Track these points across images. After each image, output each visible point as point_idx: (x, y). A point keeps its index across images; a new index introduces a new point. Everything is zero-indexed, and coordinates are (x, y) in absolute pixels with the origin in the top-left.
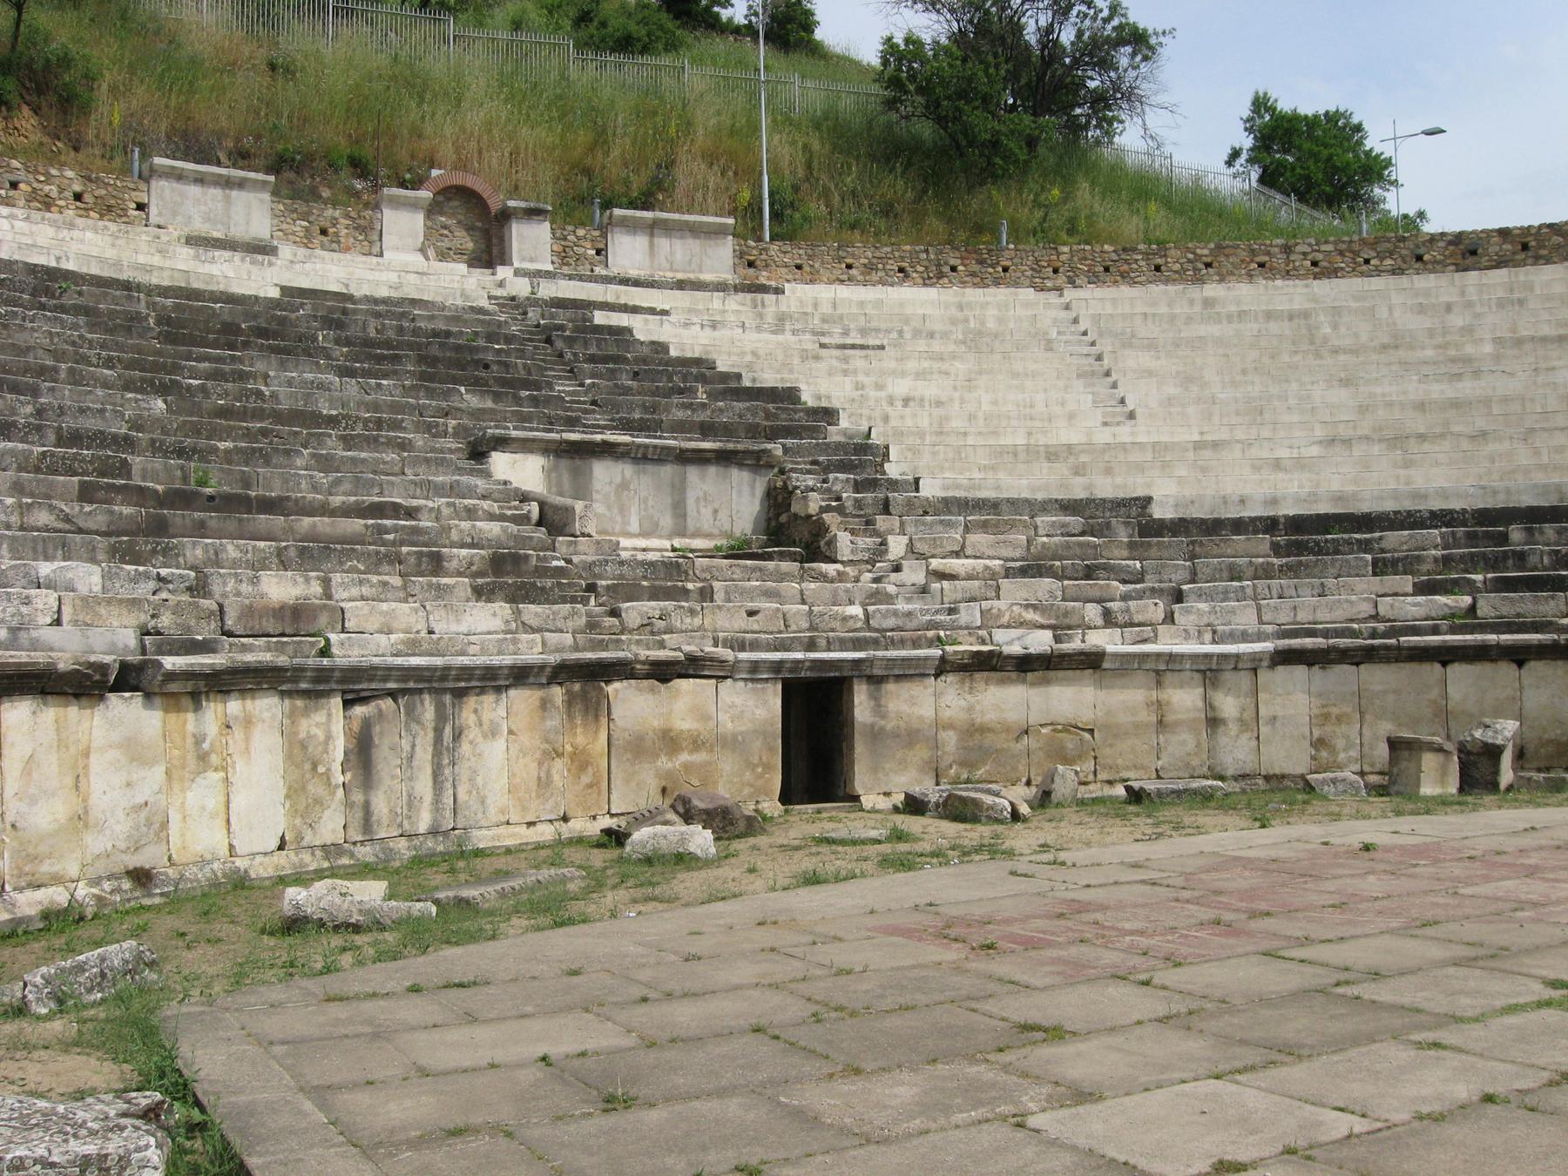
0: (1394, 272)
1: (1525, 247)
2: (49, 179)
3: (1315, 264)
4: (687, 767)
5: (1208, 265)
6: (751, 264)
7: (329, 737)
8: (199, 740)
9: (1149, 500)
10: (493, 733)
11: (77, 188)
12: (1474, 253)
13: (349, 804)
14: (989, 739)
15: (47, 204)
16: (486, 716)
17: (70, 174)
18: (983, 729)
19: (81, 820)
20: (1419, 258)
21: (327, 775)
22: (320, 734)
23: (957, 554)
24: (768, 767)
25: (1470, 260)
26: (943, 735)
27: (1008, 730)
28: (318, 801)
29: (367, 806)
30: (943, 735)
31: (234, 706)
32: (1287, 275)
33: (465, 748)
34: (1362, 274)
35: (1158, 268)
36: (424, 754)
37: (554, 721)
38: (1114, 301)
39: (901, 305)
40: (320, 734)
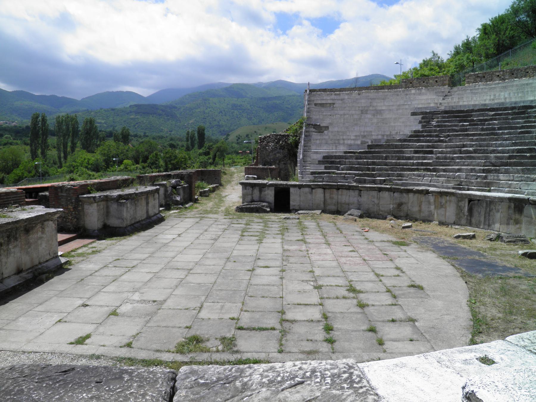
7: (465, 206)
8: (441, 203)
10: (498, 211)
13: (467, 219)
16: (497, 208)
19: (420, 211)
21: (464, 213)
22: (463, 205)
28: (461, 217)
29: (471, 220)
31: (448, 198)
33: (492, 213)
36: (483, 213)
37: (511, 211)
40: (463, 205)
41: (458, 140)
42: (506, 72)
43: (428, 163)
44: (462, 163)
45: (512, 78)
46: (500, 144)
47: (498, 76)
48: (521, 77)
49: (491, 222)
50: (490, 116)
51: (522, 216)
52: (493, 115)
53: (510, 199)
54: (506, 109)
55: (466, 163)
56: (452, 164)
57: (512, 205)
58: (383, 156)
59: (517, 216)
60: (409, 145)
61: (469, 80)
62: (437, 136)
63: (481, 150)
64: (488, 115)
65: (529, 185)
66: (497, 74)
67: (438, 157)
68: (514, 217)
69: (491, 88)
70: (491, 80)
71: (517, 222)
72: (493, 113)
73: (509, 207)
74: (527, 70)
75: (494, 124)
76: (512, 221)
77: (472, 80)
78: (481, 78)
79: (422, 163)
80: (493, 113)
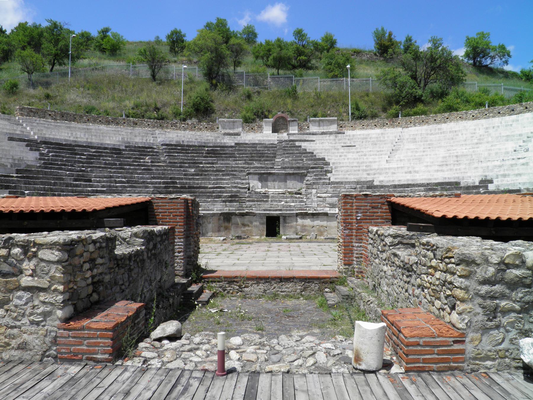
0: (493, 117)
1: (526, 108)
2: (201, 125)
3: (473, 116)
4: (247, 230)
5: (447, 118)
6: (341, 127)
9: (373, 181)
10: (210, 223)
11: (206, 126)
12: (513, 110)
14: (306, 228)
15: (201, 129)
17: (205, 124)
18: (305, 226)
20: (499, 113)
23: (325, 193)
24: (263, 231)
25: (512, 112)
26: (298, 227)
27: (310, 226)
30: (298, 227)
32: (466, 119)
34: (485, 118)
35: (435, 120)
37: (221, 222)
38: (417, 130)
39: (369, 135)
41: (98, 172)
42: (58, 113)
43: (102, 190)
44: (133, 191)
45: (63, 120)
46: (141, 177)
47: (50, 115)
48: (71, 121)
49: (204, 231)
50: (91, 152)
51: (230, 224)
52: (94, 152)
53: (221, 213)
54: (106, 148)
55: (136, 191)
56: (124, 192)
57: (222, 218)
58: (51, 183)
59: (226, 224)
60: (58, 173)
61: (23, 112)
62: (72, 166)
63: (133, 181)
64: (90, 152)
65: (214, 205)
66: (50, 113)
67: (103, 185)
68: (223, 225)
69: (56, 126)
70: (44, 117)
71: (226, 228)
72: (94, 150)
73: (219, 219)
74: (75, 117)
75: (108, 160)
76: (222, 229)
77: (26, 114)
78: (35, 113)
79: (97, 190)
80: (94, 150)
